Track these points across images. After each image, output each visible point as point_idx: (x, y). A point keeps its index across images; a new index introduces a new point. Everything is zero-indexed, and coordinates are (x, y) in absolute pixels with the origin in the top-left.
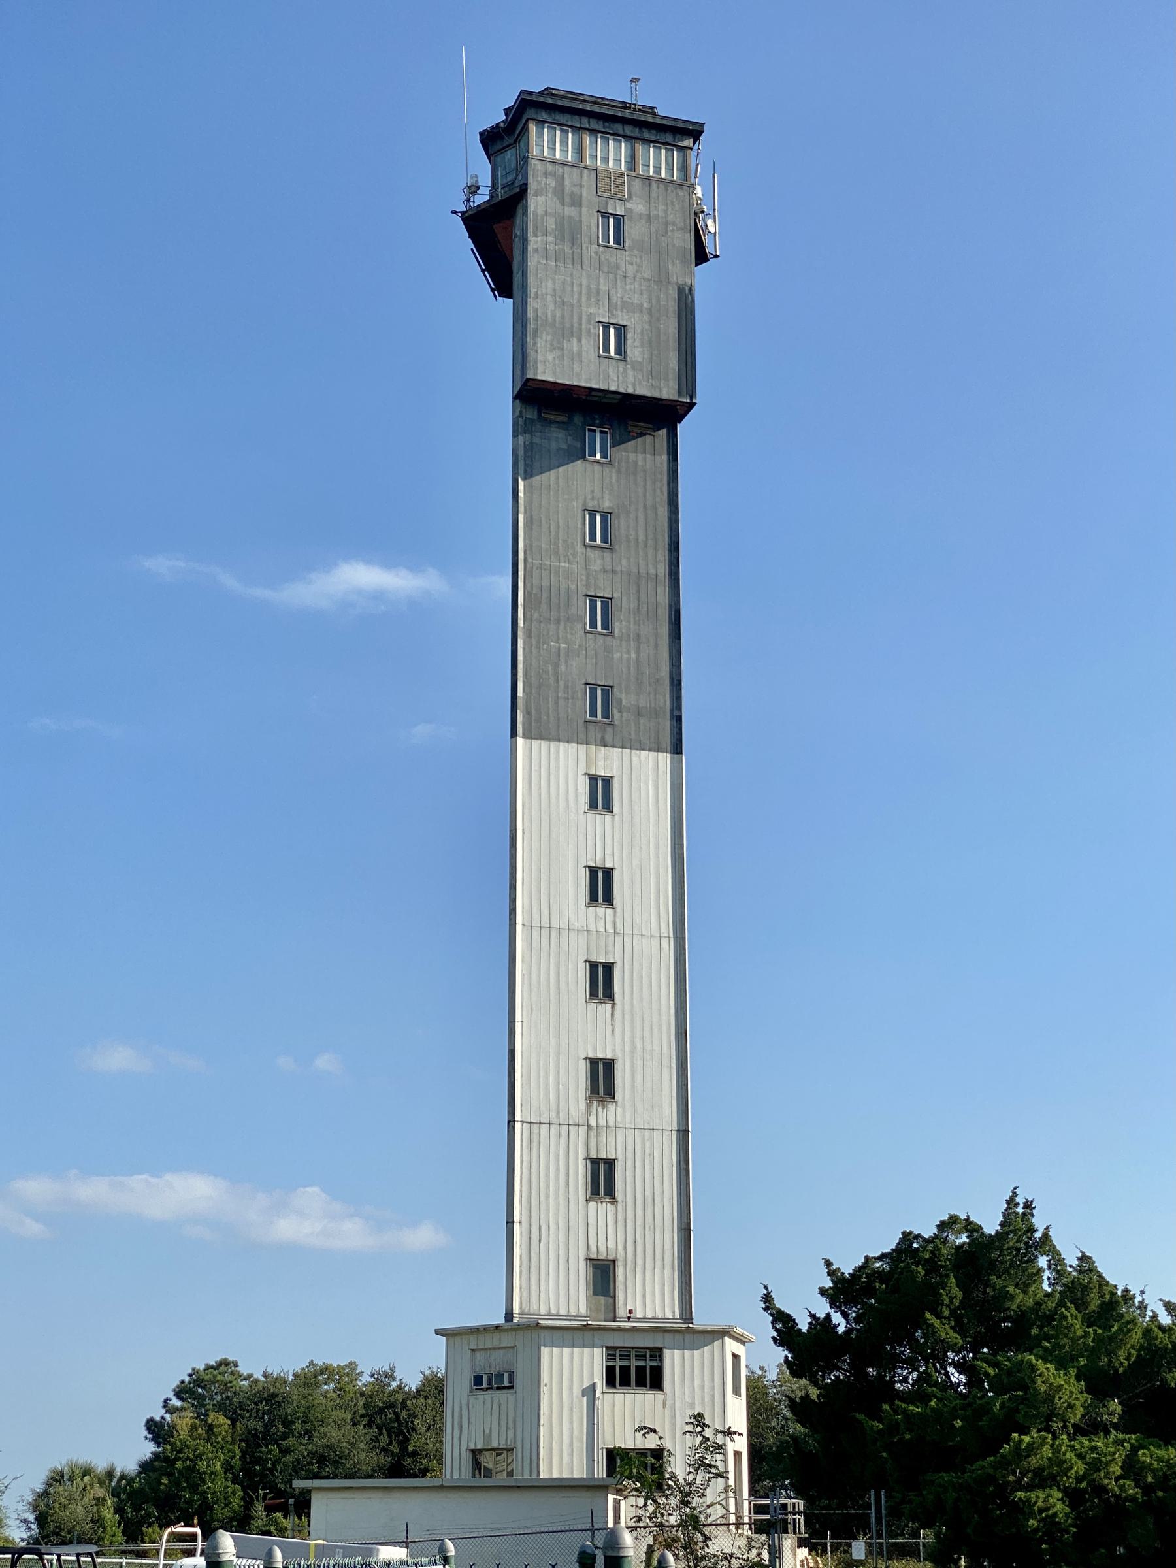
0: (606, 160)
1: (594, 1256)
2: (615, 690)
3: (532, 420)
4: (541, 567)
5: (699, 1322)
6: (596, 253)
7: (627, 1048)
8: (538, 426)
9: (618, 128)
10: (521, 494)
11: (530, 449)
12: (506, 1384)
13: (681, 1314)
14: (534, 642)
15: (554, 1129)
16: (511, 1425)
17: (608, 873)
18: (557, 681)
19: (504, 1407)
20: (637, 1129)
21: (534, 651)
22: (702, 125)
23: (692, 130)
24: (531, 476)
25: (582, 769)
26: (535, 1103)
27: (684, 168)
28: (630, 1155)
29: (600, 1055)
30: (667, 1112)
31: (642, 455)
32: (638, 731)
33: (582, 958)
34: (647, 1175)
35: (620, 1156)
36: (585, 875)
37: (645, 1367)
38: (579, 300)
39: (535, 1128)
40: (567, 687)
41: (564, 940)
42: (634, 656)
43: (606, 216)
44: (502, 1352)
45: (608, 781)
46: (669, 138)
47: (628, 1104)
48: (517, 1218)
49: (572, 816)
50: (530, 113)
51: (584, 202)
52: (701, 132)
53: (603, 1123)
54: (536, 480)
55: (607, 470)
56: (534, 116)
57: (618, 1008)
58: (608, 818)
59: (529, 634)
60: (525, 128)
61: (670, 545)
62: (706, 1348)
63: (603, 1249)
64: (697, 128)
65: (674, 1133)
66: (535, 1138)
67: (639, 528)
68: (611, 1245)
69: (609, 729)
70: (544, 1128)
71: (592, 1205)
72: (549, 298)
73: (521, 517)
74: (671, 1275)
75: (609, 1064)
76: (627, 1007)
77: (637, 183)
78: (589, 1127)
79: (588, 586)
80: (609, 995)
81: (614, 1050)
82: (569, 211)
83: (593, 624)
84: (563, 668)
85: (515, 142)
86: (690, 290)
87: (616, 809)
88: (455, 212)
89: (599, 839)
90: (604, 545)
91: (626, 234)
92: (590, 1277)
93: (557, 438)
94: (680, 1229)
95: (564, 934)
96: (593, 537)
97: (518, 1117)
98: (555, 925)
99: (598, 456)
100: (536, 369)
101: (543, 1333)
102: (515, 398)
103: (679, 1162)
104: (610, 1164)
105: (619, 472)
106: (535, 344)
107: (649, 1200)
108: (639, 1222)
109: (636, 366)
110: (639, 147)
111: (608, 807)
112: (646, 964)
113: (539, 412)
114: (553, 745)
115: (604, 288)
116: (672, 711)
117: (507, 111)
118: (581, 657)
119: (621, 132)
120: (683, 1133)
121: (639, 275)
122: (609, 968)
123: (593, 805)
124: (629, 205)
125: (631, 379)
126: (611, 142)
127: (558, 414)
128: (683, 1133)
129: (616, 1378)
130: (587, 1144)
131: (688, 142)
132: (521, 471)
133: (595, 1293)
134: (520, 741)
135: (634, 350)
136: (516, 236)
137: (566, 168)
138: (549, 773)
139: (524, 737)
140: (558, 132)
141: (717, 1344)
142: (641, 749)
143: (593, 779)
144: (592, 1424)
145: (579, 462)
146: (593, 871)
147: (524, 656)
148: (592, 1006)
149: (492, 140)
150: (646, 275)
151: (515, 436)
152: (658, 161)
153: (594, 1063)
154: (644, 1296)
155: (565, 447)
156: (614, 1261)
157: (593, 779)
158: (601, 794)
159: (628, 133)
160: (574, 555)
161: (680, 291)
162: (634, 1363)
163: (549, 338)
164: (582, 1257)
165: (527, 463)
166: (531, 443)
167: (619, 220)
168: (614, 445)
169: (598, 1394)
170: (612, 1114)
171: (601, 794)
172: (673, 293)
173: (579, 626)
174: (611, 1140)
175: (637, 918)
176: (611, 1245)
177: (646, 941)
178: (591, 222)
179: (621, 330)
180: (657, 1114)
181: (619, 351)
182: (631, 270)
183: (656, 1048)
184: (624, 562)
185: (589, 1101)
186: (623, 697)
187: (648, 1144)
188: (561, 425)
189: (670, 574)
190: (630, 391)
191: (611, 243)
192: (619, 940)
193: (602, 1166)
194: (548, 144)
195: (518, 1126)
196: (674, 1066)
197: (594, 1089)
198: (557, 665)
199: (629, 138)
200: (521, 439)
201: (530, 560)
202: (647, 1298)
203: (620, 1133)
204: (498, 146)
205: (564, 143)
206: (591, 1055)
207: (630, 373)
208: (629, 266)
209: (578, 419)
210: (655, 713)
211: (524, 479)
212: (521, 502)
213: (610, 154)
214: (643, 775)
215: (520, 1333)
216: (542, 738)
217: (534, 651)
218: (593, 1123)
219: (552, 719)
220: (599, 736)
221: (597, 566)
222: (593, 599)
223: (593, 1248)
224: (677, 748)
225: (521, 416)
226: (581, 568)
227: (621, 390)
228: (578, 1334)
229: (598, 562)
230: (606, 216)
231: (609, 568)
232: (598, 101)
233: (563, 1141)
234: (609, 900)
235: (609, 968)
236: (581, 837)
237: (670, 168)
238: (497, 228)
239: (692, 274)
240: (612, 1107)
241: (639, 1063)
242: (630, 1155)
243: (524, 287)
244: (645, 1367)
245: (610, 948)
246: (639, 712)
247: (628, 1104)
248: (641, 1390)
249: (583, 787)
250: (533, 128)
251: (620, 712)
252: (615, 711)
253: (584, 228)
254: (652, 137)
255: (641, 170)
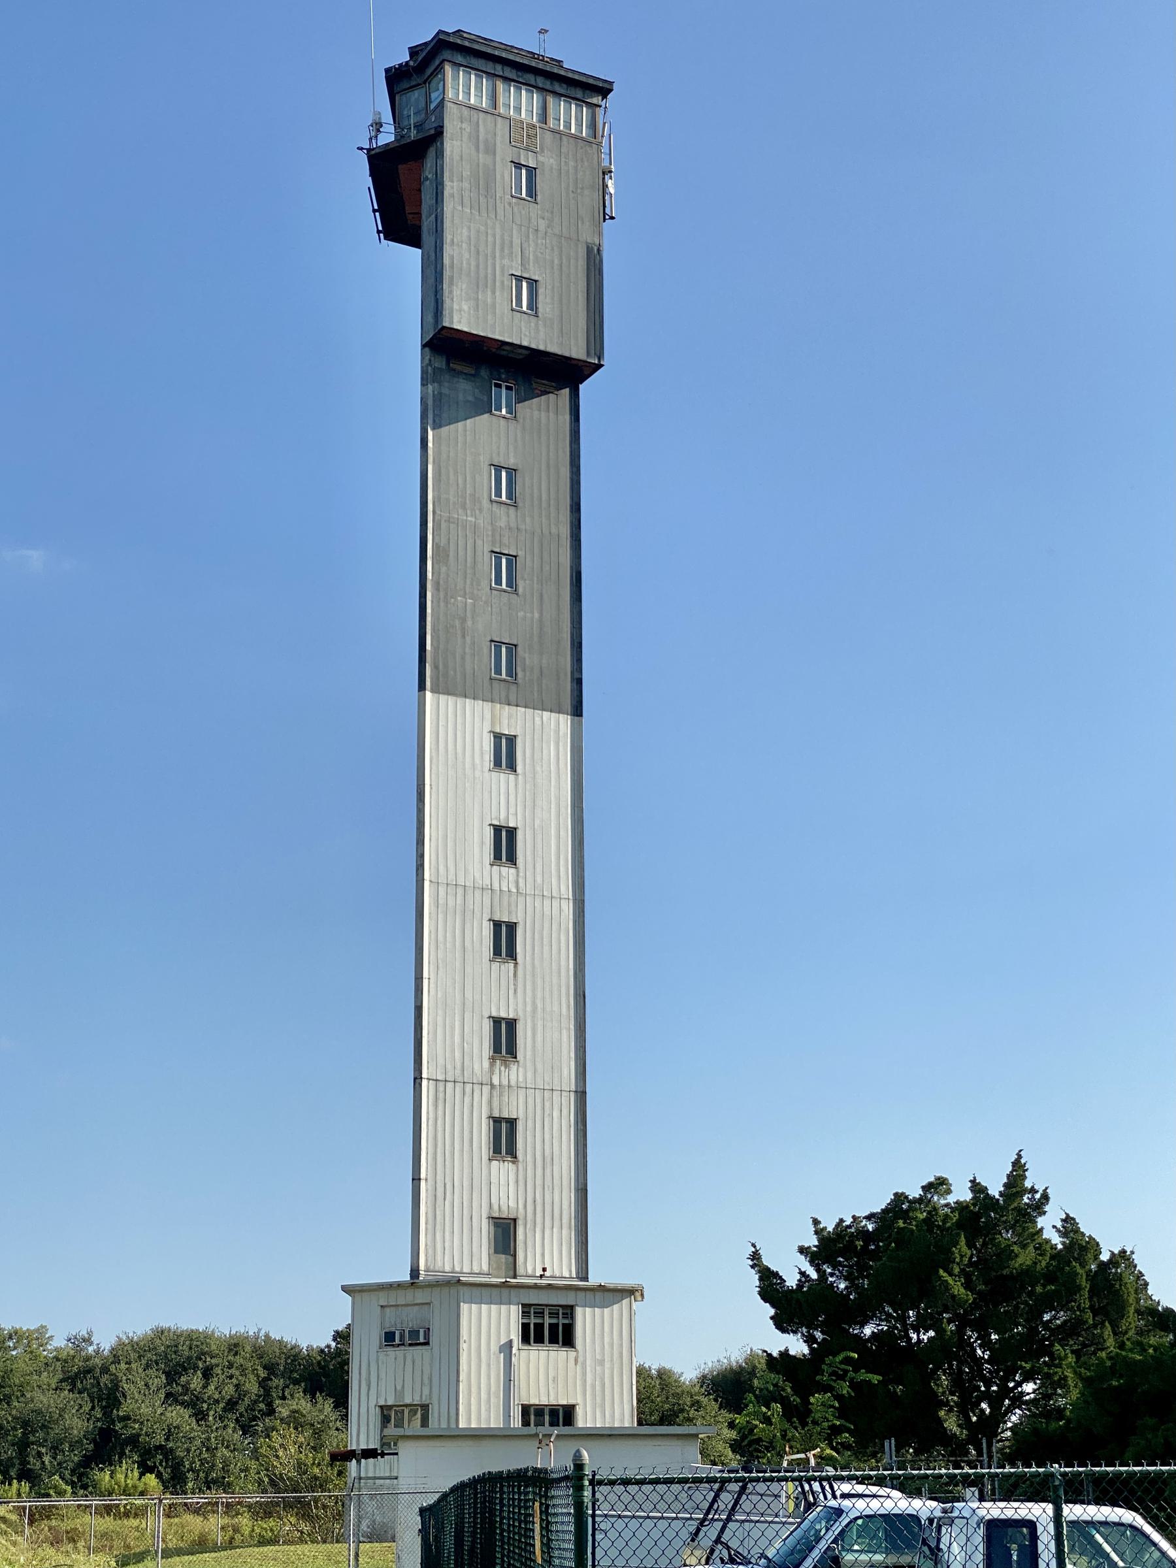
0: (518, 109)
1: (496, 1215)
2: (519, 649)
3: (440, 369)
4: (448, 521)
5: (594, 1279)
6: (510, 204)
7: (529, 1008)
8: (447, 377)
9: (530, 78)
10: (430, 445)
11: (439, 399)
12: (422, 1340)
13: (577, 1273)
14: (442, 595)
15: (459, 1086)
16: (426, 1381)
17: (512, 832)
18: (464, 636)
19: (418, 1363)
20: (537, 1086)
21: (442, 604)
22: (611, 83)
23: (602, 88)
24: (440, 427)
25: (487, 727)
26: (441, 1061)
27: (593, 125)
28: (530, 1115)
29: (503, 1015)
30: (565, 1072)
31: (545, 411)
32: (540, 692)
33: (486, 916)
34: (547, 1135)
35: (521, 1116)
36: (489, 833)
37: (557, 1324)
38: (494, 252)
39: (441, 1085)
40: (473, 643)
41: (469, 897)
42: (536, 615)
43: (518, 166)
44: (416, 1308)
45: (511, 740)
46: (579, 95)
47: (529, 1064)
48: (423, 1176)
49: (478, 773)
50: (447, 54)
51: (498, 151)
52: (611, 90)
53: (505, 1082)
54: (444, 430)
55: (512, 424)
56: (449, 58)
57: (520, 968)
58: (512, 777)
59: (437, 585)
60: (439, 69)
61: (571, 506)
62: (616, 1307)
63: (504, 1208)
64: (606, 86)
65: (572, 1095)
66: (441, 1095)
67: (544, 485)
68: (512, 1204)
69: (513, 688)
70: (450, 1085)
71: (494, 1163)
72: (464, 245)
73: (430, 467)
74: (568, 1235)
75: (512, 1024)
76: (529, 967)
77: (548, 135)
78: (492, 1086)
79: (493, 543)
80: (512, 955)
81: (516, 1010)
82: (483, 158)
83: (498, 581)
84: (469, 623)
85: (425, 83)
86: (599, 250)
87: (519, 768)
88: (361, 149)
89: (502, 798)
90: (509, 501)
91: (538, 187)
92: (492, 1236)
93: (464, 389)
94: (577, 1190)
95: (470, 892)
96: (499, 494)
97: (424, 1075)
98: (461, 882)
99: (504, 411)
100: (452, 318)
101: (462, 1290)
102: (424, 346)
103: (576, 1123)
104: (512, 1123)
105: (524, 428)
106: (451, 292)
107: (548, 1160)
108: (539, 1182)
110: (551, 100)
111: (512, 766)
112: (547, 925)
113: (448, 363)
114: (460, 701)
115: (516, 241)
116: (572, 673)
117: (414, 52)
118: (486, 616)
119: (533, 82)
120: (581, 1095)
121: (549, 230)
122: (512, 927)
123: (497, 763)
124: (541, 158)
125: (542, 334)
126: (523, 92)
127: (468, 365)
128: (581, 1095)
129: (532, 1334)
130: (490, 1102)
131: (596, 100)
132: (430, 421)
133: (496, 1252)
134: (428, 695)
136: (427, 179)
137: (481, 114)
139: (432, 691)
140: (473, 77)
141: (625, 1302)
142: (543, 710)
143: (498, 737)
144: (508, 1380)
145: (486, 416)
146: (497, 830)
147: (433, 609)
148: (495, 966)
149: (396, 79)
150: (557, 231)
151: (424, 382)
152: (569, 115)
153: (497, 1021)
154: (543, 1255)
155: (470, 398)
156: (515, 1220)
157: (498, 737)
158: (505, 754)
159: (541, 85)
160: (481, 510)
161: (589, 250)
162: (547, 1321)
163: (464, 286)
164: (484, 1216)
165: (435, 413)
166: (440, 394)
167: (532, 171)
168: (520, 400)
169: (514, 1350)
170: (514, 1073)
171: (505, 754)
172: (582, 252)
173: (486, 582)
174: (513, 1098)
175: (539, 879)
176: (512, 1204)
177: (547, 902)
178: (505, 174)
179: (533, 283)
180: (556, 1075)
181: (530, 307)
182: (542, 224)
183: (556, 1008)
184: (528, 520)
185: (492, 1059)
186: (527, 655)
187: (547, 1104)
188: (468, 376)
189: (572, 536)
190: (542, 348)
191: (524, 195)
192: (521, 899)
193: (504, 1125)
194: (462, 88)
195: (424, 1083)
196: (572, 1027)
197: (497, 1049)
198: (464, 620)
199: (540, 89)
200: (430, 387)
201: (438, 512)
202: (546, 1256)
203: (522, 1092)
204: (405, 85)
205: (479, 88)
206: (494, 1014)
207: (541, 328)
208: (541, 221)
209: (484, 373)
211: (433, 429)
212: (430, 452)
213: (522, 103)
214: (546, 734)
215: (436, 1291)
216: (448, 694)
217: (442, 604)
218: (496, 1081)
219: (458, 674)
220: (503, 694)
221: (502, 523)
222: (498, 555)
223: (496, 1207)
225: (430, 364)
227: (533, 346)
228: (495, 1291)
229: (505, 517)
230: (518, 166)
231: (513, 525)
232: (509, 48)
233: (467, 1100)
234: (512, 859)
235: (512, 927)
236: (486, 795)
237: (579, 125)
238: (402, 168)
239: (600, 234)
240: (514, 1067)
241: (540, 1023)
242: (530, 1115)
243: (438, 230)
244: (557, 1324)
245: (513, 908)
247: (529, 1064)
248: (555, 1347)
249: (488, 744)
250: (448, 69)
251: (524, 670)
252: (519, 669)
253: (498, 177)
254: (562, 91)
255: (551, 123)
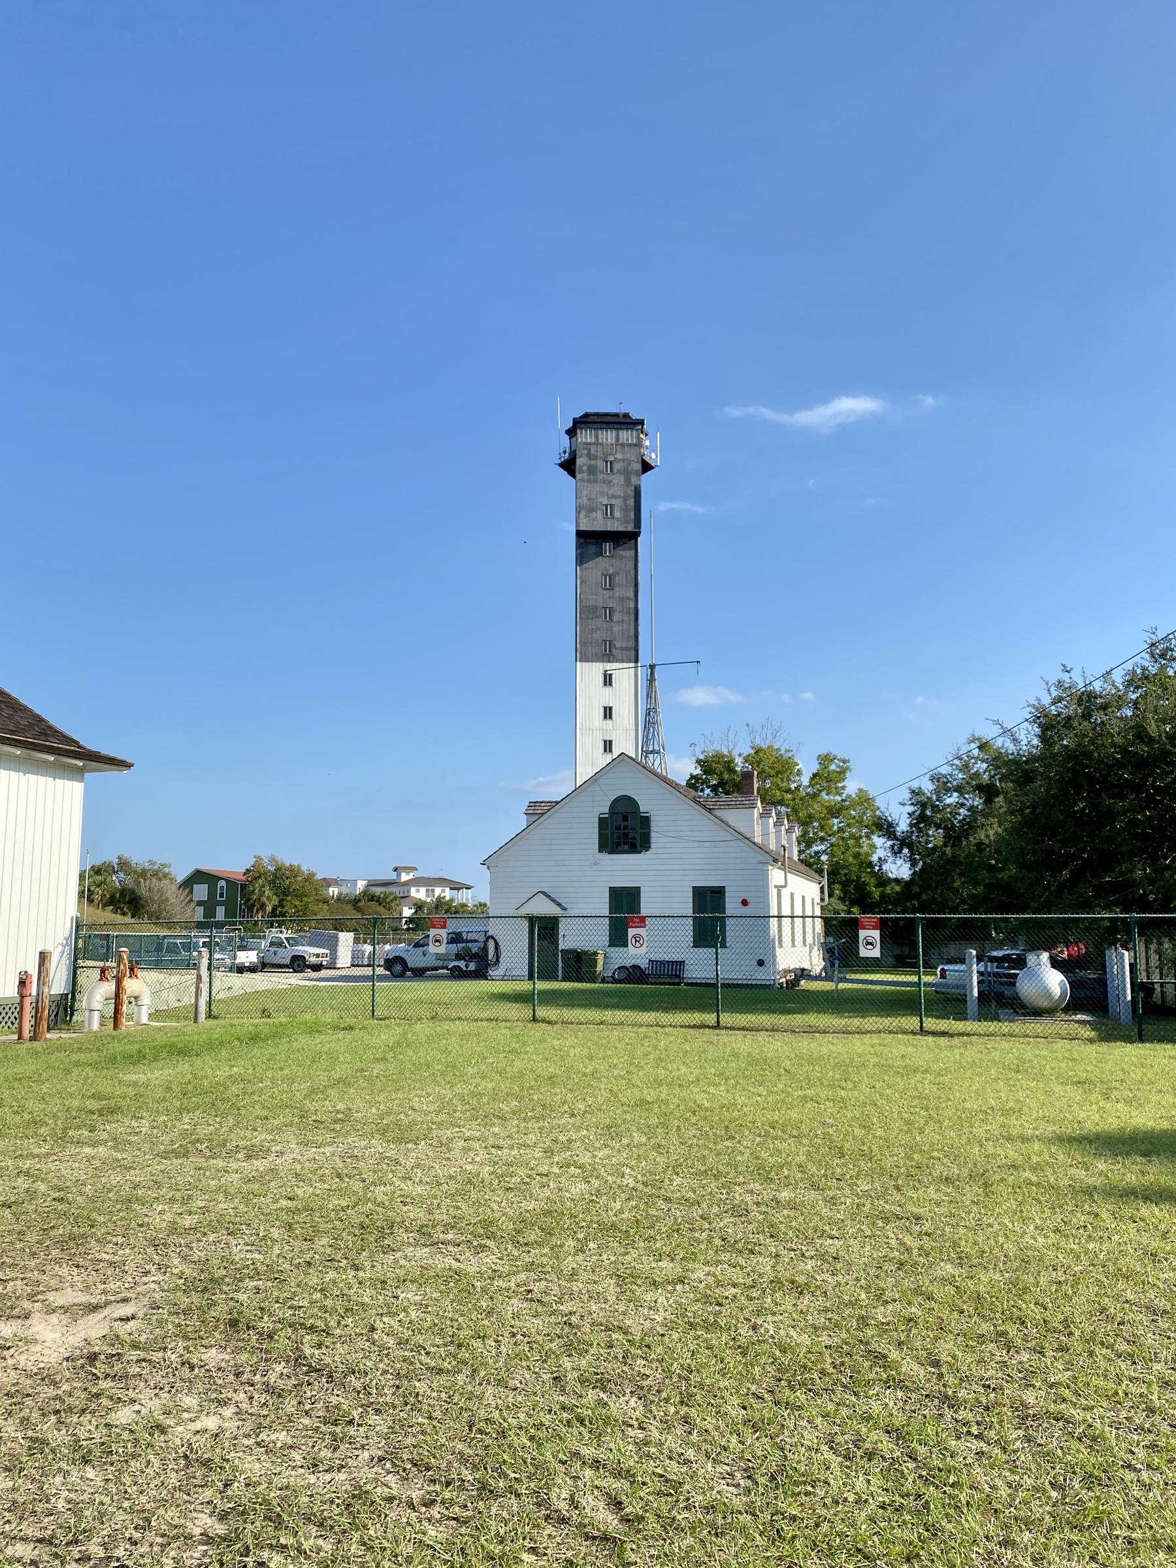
36: (602, 710)
89: (606, 696)
109: (618, 520)
122: (611, 742)
135: (617, 514)
138: (590, 673)
146: (605, 708)
171: (608, 680)
179: (611, 506)
210: (628, 649)
214: (624, 674)
224: (636, 661)
226: (601, 598)
246: (622, 649)
